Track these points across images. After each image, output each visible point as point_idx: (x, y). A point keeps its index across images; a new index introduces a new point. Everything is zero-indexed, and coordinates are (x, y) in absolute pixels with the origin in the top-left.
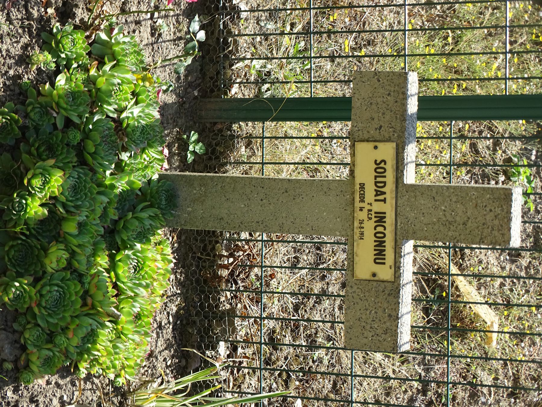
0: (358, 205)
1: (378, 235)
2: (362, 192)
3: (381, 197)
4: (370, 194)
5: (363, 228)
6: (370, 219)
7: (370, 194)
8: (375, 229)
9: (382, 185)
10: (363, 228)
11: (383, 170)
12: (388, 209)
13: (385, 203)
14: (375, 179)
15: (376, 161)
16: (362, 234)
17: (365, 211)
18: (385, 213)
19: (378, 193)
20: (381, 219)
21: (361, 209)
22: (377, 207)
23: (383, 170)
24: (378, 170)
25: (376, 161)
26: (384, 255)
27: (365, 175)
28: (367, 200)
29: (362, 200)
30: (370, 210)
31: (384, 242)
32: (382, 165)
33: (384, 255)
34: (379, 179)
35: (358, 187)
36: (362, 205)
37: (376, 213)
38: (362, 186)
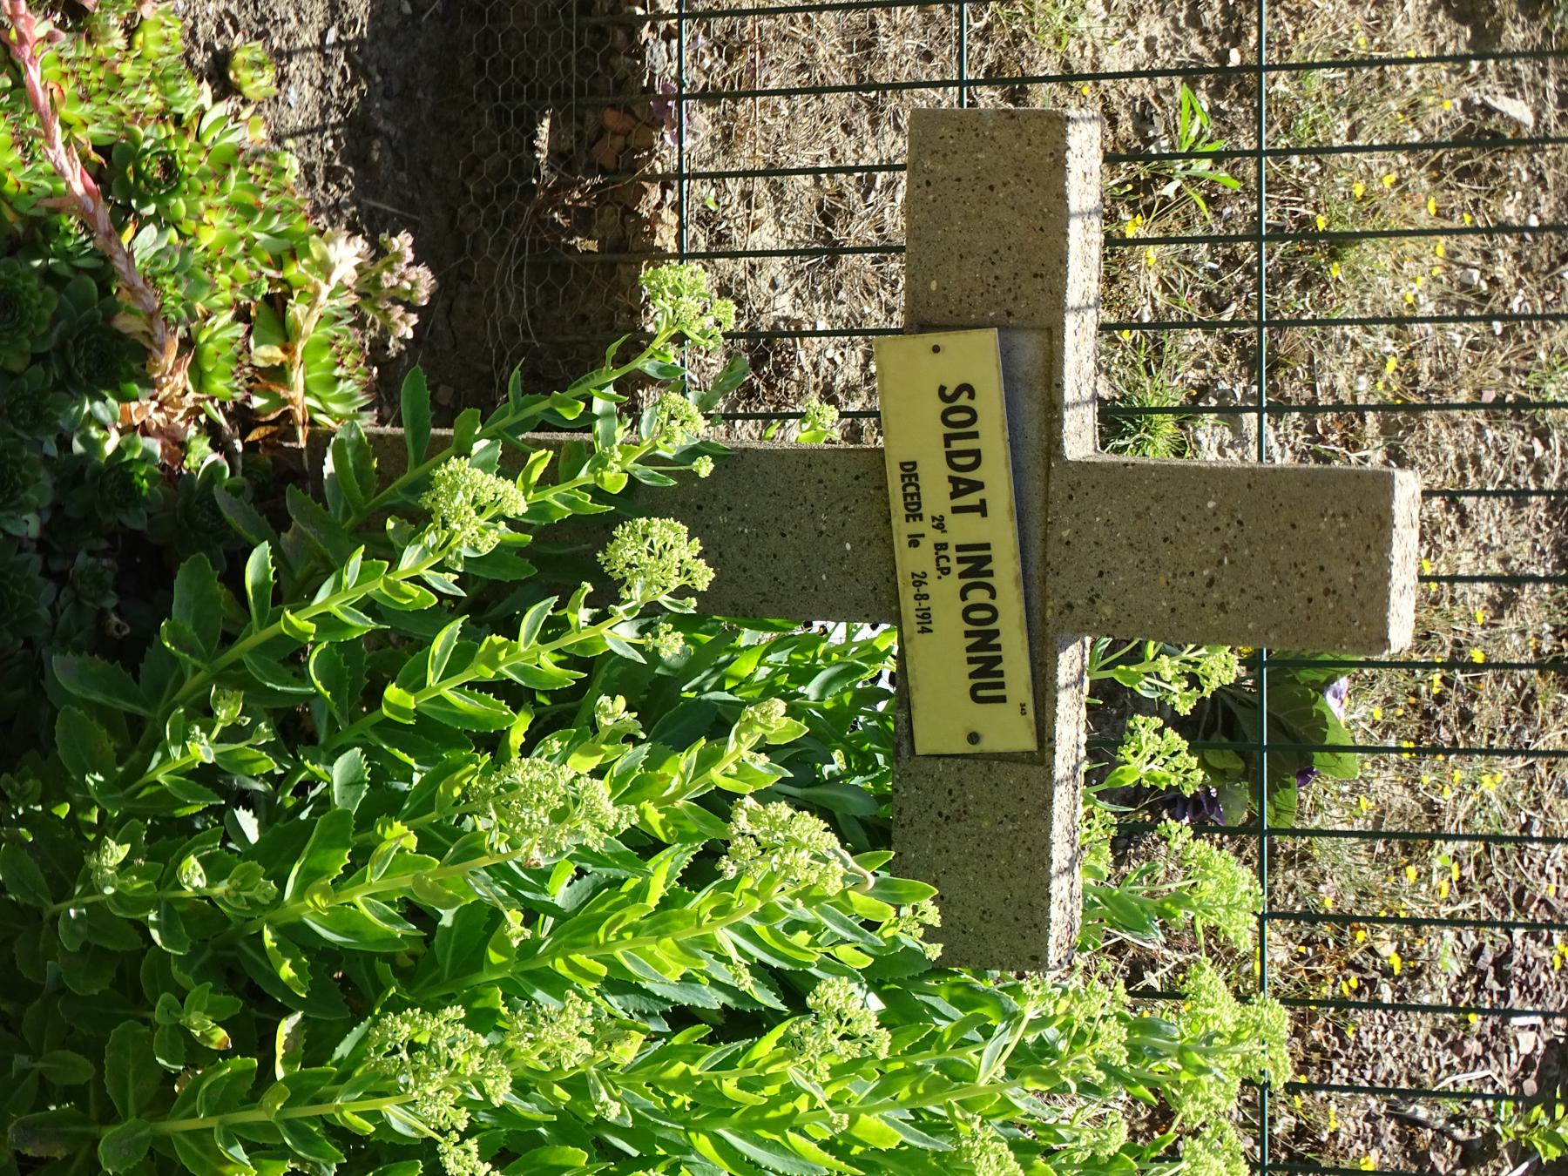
0: (902, 528)
1: (974, 615)
2: (911, 489)
3: (972, 499)
4: (936, 495)
5: (926, 597)
6: (946, 571)
7: (936, 495)
8: (964, 598)
9: (969, 460)
10: (926, 597)
11: (965, 417)
12: (998, 531)
13: (984, 514)
14: (947, 445)
15: (942, 389)
16: (925, 616)
17: (927, 546)
18: (987, 546)
19: (960, 487)
20: (977, 563)
21: (914, 542)
22: (965, 529)
23: (965, 417)
24: (954, 417)
25: (942, 389)
26: (1001, 674)
27: (916, 437)
28: (928, 510)
29: (914, 514)
31: (996, 633)
32: (963, 400)
33: (1001, 674)
34: (957, 445)
36: (915, 527)
37: (959, 548)
38: (910, 471)
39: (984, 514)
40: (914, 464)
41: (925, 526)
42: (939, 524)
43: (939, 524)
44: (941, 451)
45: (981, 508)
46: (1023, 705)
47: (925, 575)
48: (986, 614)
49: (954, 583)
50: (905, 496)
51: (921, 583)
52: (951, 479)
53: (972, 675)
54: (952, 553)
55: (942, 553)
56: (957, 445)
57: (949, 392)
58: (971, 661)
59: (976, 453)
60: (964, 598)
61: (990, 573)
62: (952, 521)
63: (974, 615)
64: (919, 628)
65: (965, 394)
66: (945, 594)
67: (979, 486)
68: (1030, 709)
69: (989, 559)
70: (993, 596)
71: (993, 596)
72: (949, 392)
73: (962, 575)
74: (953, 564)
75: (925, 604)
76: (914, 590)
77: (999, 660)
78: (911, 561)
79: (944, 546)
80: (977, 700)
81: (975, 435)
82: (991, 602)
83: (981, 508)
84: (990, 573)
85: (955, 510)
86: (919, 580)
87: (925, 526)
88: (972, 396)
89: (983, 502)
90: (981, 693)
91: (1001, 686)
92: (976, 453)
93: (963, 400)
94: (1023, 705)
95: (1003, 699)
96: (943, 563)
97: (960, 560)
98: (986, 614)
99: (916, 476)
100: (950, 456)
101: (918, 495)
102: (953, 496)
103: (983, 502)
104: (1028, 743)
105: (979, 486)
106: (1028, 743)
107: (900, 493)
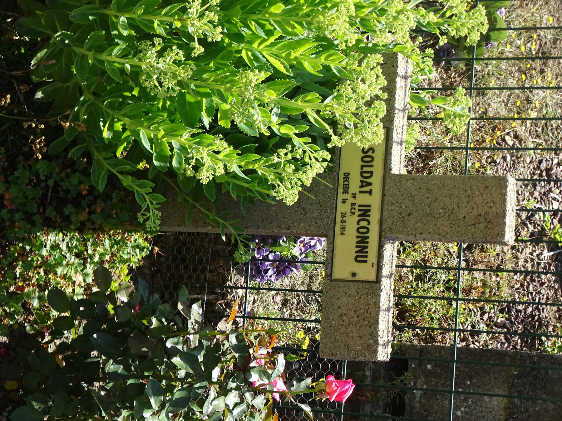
0: (341, 196)
1: (361, 230)
2: (346, 183)
3: (367, 189)
4: (354, 186)
5: (345, 222)
6: (353, 213)
7: (355, 185)
8: (358, 224)
10: (345, 222)
11: (369, 159)
12: (374, 201)
13: (371, 195)
14: (362, 169)
16: (343, 228)
17: (348, 203)
18: (370, 206)
19: (364, 184)
20: (365, 212)
21: (344, 201)
22: (363, 199)
23: (369, 159)
28: (351, 191)
29: (346, 192)
30: (353, 204)
31: (368, 237)
32: (370, 153)
33: (367, 252)
34: (365, 169)
35: (341, 177)
36: (345, 196)
37: (360, 206)
38: (347, 176)
39: (371, 195)
40: (349, 174)
41: (349, 196)
42: (354, 196)
43: (354, 196)
44: (359, 170)
45: (370, 192)
46: (373, 264)
47: (346, 213)
48: (365, 230)
49: (356, 218)
50: (344, 185)
51: (344, 216)
52: (361, 181)
53: (356, 252)
54: (357, 207)
55: (353, 207)
56: (365, 169)
57: (365, 150)
58: (357, 247)
59: (371, 173)
60: (358, 224)
61: (369, 216)
62: (359, 196)
63: (361, 230)
64: (340, 233)
65: (371, 151)
66: (352, 222)
67: (370, 184)
68: (375, 266)
69: (369, 210)
70: (369, 224)
71: (369, 224)
72: (365, 150)
73: (359, 216)
74: (356, 211)
75: (344, 224)
76: (341, 219)
77: (367, 247)
78: (342, 208)
79: (354, 204)
80: (357, 261)
81: (372, 166)
82: (368, 226)
83: (370, 192)
84: (369, 216)
85: (361, 192)
86: (343, 215)
87: (349, 196)
88: (373, 152)
89: (371, 190)
90: (358, 259)
91: (366, 257)
92: (371, 173)
93: (370, 153)
94: (373, 264)
95: (366, 262)
96: (353, 210)
97: (359, 210)
98: (365, 230)
99: (349, 178)
100: (362, 173)
101: (348, 185)
102: (361, 187)
103: (371, 190)
104: (373, 277)
105: (370, 184)
106: (373, 277)
107: (342, 184)
